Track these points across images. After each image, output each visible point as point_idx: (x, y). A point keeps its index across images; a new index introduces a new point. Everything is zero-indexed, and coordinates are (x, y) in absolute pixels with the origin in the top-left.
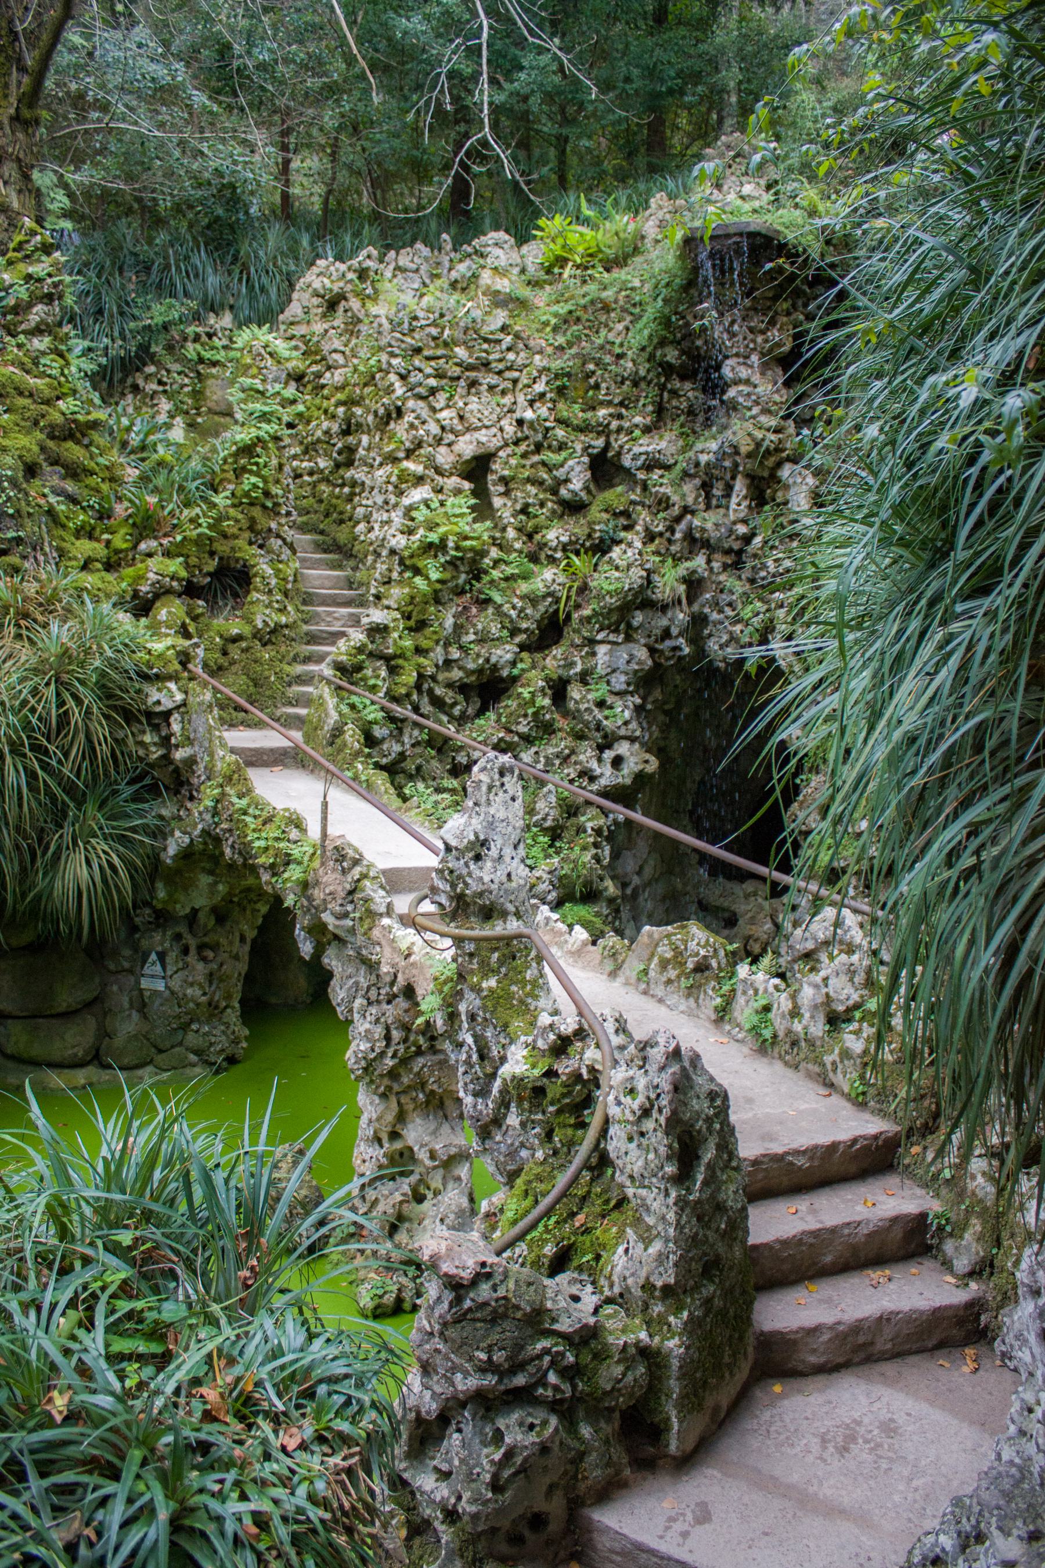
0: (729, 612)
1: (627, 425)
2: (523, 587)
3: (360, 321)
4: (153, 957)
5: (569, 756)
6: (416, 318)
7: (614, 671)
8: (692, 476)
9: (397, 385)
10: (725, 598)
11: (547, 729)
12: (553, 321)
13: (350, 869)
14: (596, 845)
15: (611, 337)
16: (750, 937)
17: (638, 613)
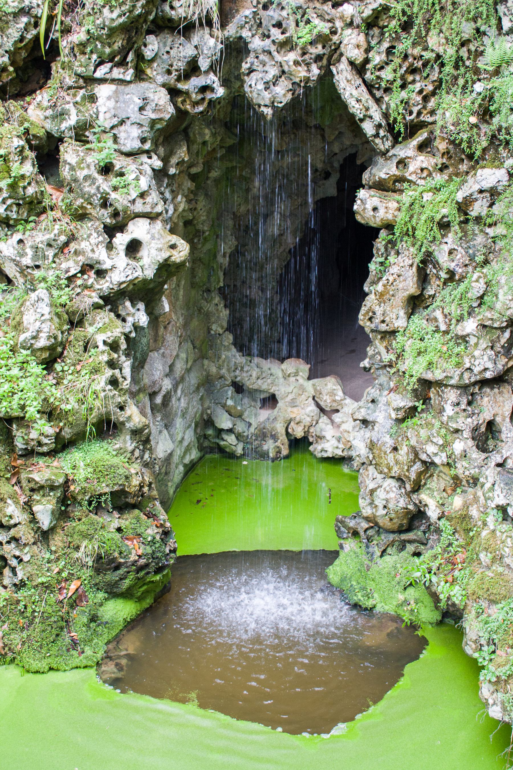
5: (66, 244)
7: (122, 122)
11: (35, 207)
14: (112, 364)
16: (291, 420)
17: (151, 38)
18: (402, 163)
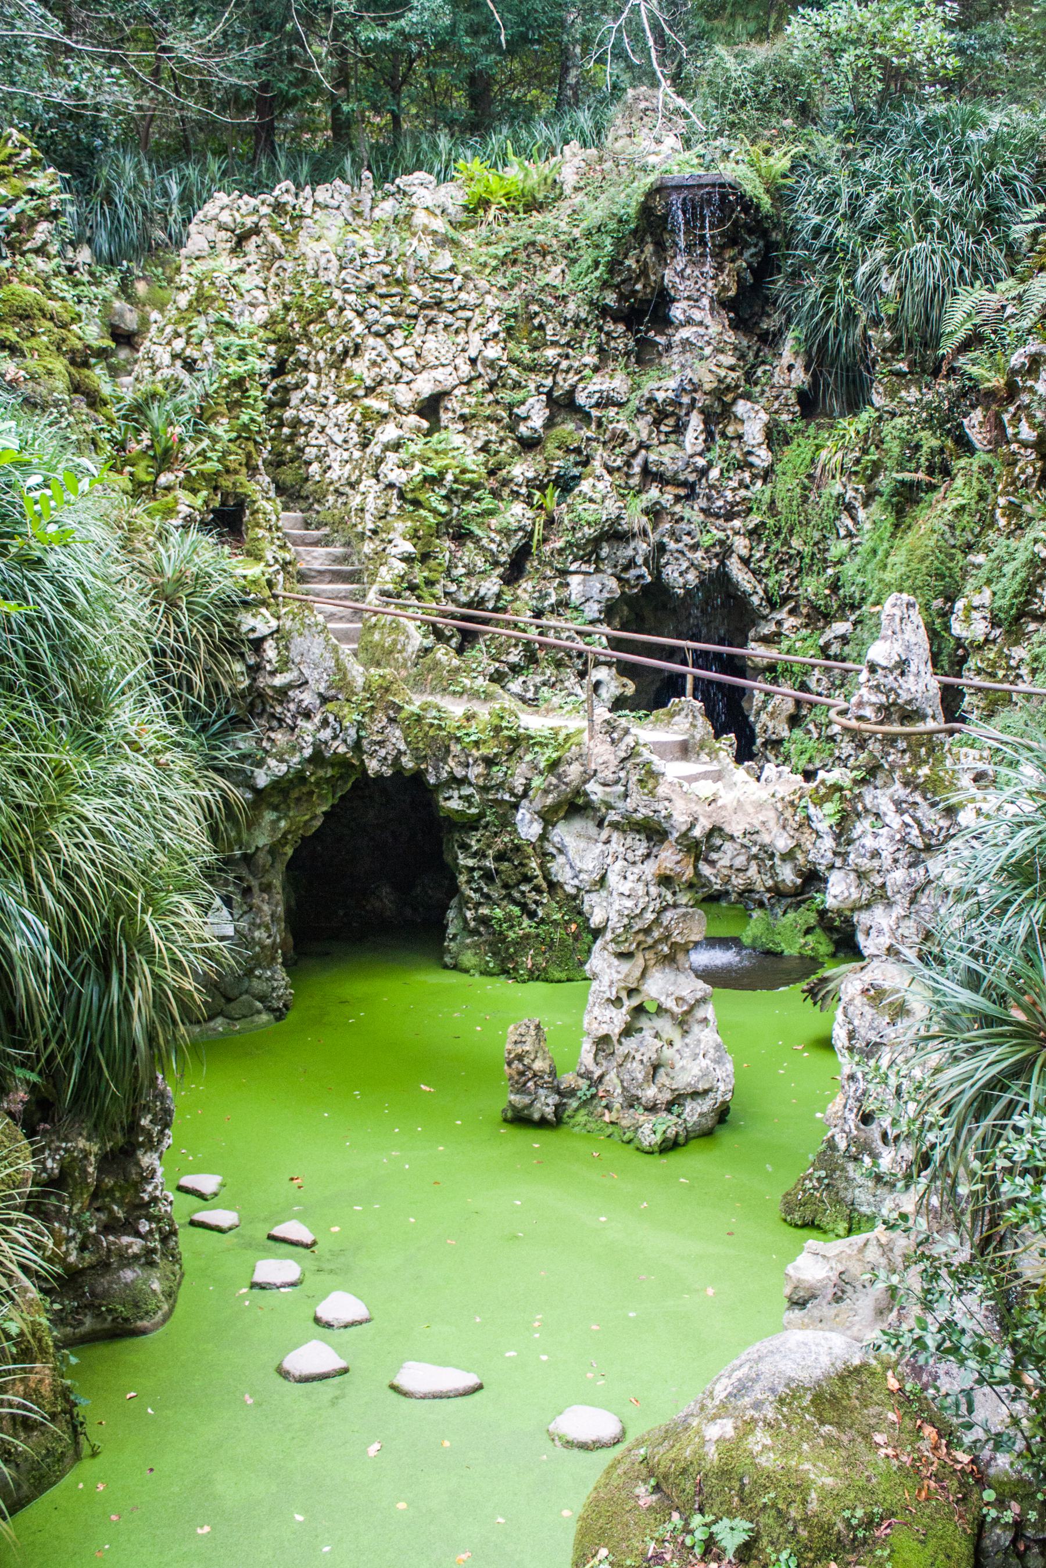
0: (687, 539)
1: (576, 364)
2: (494, 522)
3: (281, 257)
6: (364, 255)
8: (645, 413)
9: (356, 322)
10: (683, 525)
12: (494, 263)
13: (621, 739)
15: (548, 278)
18: (779, 623)
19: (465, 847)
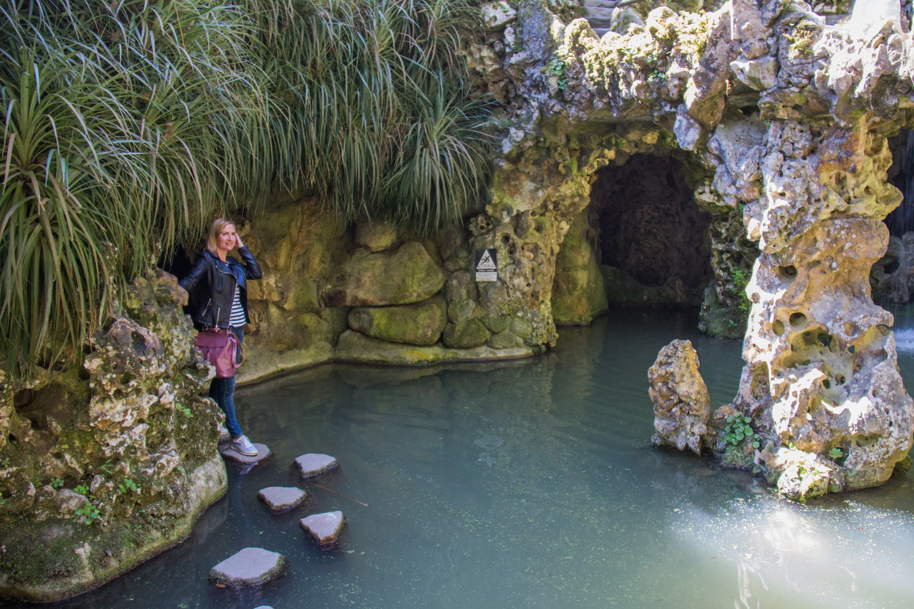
4: (486, 254)
19: (717, 235)
